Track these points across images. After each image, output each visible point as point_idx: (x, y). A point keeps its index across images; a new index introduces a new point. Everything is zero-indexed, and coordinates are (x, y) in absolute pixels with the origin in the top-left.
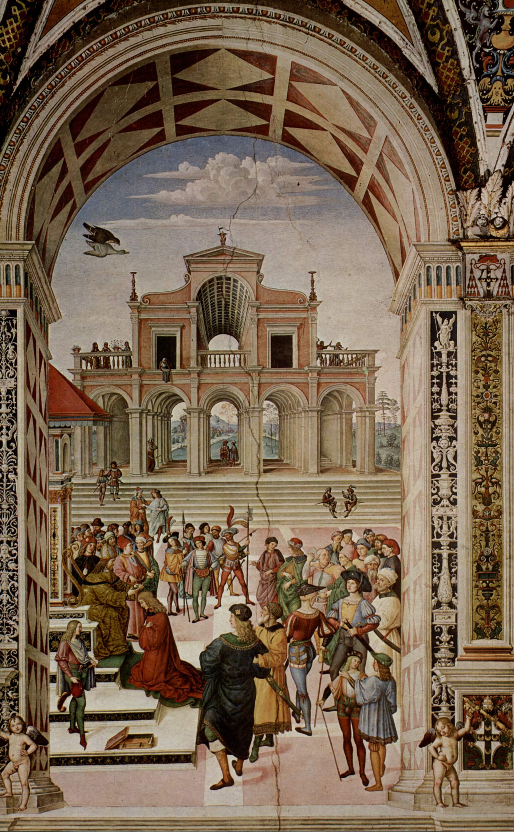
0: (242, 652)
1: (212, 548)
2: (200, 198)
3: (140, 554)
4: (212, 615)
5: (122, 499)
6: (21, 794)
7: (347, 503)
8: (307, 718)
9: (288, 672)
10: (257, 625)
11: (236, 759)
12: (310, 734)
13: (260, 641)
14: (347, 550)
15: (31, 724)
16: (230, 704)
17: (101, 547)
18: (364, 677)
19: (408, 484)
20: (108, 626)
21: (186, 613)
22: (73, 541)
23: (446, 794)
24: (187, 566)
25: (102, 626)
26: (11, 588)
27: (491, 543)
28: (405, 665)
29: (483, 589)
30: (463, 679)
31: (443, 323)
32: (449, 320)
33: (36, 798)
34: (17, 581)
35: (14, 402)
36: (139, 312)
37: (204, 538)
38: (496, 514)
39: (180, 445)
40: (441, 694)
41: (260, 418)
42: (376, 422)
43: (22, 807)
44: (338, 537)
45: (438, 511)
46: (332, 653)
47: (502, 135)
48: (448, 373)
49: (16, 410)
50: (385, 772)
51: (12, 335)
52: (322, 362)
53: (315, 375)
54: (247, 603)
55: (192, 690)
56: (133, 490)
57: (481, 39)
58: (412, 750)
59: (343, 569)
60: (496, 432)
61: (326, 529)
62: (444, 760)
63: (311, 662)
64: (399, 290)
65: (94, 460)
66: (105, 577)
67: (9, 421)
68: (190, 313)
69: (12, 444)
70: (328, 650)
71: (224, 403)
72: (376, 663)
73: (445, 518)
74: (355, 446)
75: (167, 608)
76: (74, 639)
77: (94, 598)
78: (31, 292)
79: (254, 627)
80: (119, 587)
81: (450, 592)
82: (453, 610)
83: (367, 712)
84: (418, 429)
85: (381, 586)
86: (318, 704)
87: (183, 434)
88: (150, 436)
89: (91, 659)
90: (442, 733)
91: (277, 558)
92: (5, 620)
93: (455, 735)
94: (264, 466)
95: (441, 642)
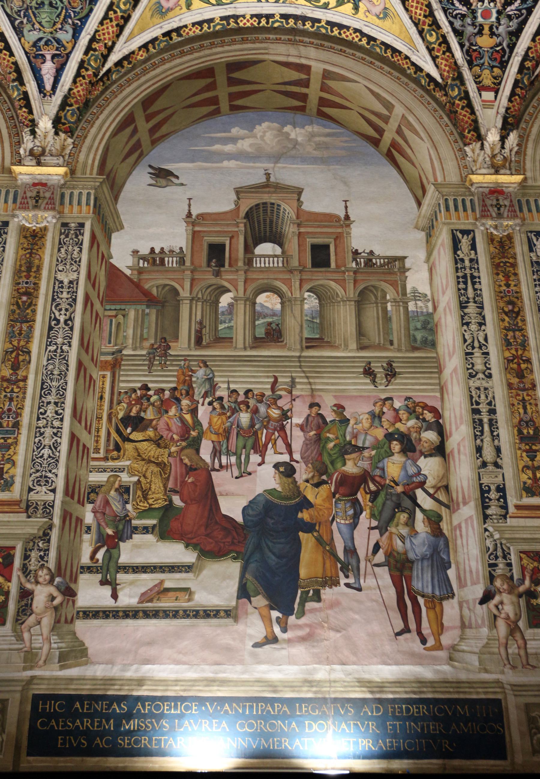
0: (286, 507)
1: (256, 411)
2: (249, 150)
3: (185, 415)
4: (255, 472)
5: (169, 368)
6: (41, 648)
7: (386, 375)
8: (356, 572)
9: (334, 526)
10: (302, 482)
11: (280, 615)
12: (359, 589)
13: (305, 498)
14: (389, 415)
15: (59, 575)
16: (273, 557)
17: (147, 408)
18: (413, 533)
19: (444, 360)
20: (149, 481)
21: (229, 470)
22: (119, 403)
23: (513, 654)
24: (231, 426)
25: (142, 479)
26: (54, 443)
27: (529, 411)
28: (455, 523)
29: (527, 451)
30: (517, 536)
31: (463, 237)
32: (468, 236)
33: (57, 653)
34: (60, 437)
35: (75, 290)
36: (193, 226)
37: (248, 402)
38: (530, 386)
39: (226, 325)
40: (496, 550)
41: (302, 305)
42: (410, 309)
43: (41, 663)
44: (380, 403)
45: (474, 383)
46: (380, 508)
47: (496, 108)
48: (471, 274)
49: (76, 296)
50: (444, 631)
51: (79, 240)
52: (357, 264)
53: (352, 274)
54: (291, 461)
55: (233, 543)
56: (182, 360)
57: (469, 40)
58: (471, 608)
59: (386, 432)
60: (521, 320)
61: (369, 397)
62: (508, 618)
63: (359, 518)
64: (422, 214)
65: (145, 336)
66: (149, 436)
67: (68, 304)
68: (238, 227)
69: (69, 322)
70: (376, 506)
71: (268, 294)
72: (426, 520)
73: (482, 389)
74: (392, 329)
75: (210, 464)
76: (113, 493)
77: (136, 454)
78: (99, 211)
79: (298, 483)
80: (163, 445)
81: (494, 453)
82: (499, 470)
83: (420, 567)
84: (449, 318)
85: (425, 447)
86: (368, 560)
87: (230, 316)
88: (199, 318)
89: (129, 511)
90: (501, 590)
91: (320, 421)
92: (44, 473)
93: (516, 592)
94: (306, 343)
95: (490, 500)
